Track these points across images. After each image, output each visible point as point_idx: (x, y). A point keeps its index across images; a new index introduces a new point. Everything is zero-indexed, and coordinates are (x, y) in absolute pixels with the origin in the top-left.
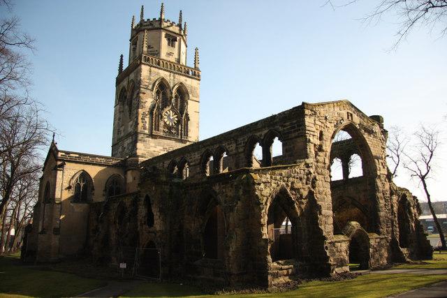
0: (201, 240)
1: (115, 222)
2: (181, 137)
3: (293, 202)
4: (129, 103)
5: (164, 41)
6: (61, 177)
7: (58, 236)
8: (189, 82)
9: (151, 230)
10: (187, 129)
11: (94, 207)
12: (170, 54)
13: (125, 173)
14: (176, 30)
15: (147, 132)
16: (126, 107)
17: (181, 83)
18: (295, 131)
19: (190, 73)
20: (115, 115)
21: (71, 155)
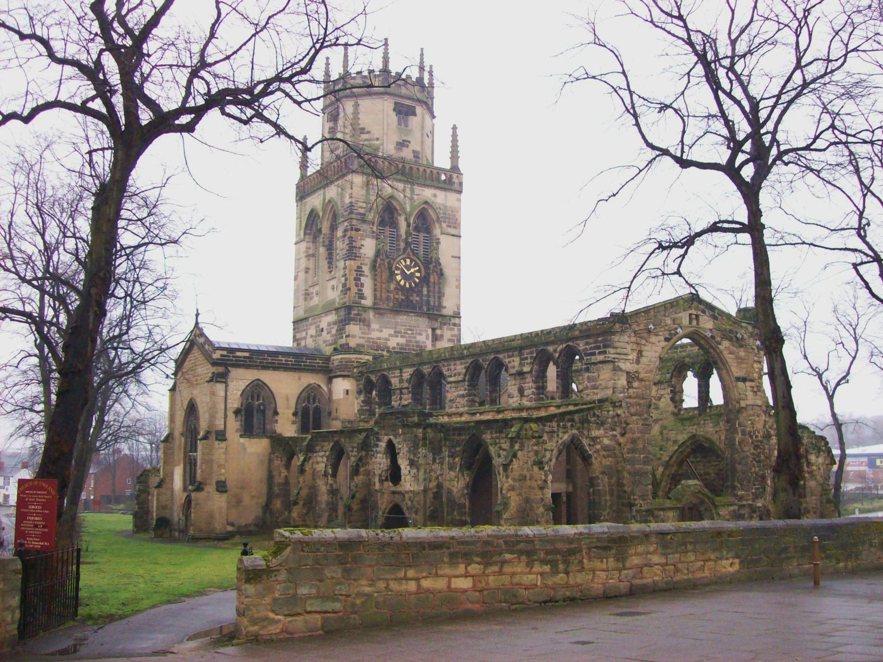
0: (467, 504)
1: (326, 474)
2: (428, 310)
3: (590, 456)
4: (327, 243)
5: (393, 117)
6: (222, 394)
7: (225, 495)
8: (440, 198)
9: (398, 488)
10: (439, 292)
11: (279, 443)
13: (330, 381)
15: (368, 302)
16: (322, 250)
17: (426, 203)
18: (600, 353)
19: (443, 177)
20: (298, 260)
21: (238, 354)
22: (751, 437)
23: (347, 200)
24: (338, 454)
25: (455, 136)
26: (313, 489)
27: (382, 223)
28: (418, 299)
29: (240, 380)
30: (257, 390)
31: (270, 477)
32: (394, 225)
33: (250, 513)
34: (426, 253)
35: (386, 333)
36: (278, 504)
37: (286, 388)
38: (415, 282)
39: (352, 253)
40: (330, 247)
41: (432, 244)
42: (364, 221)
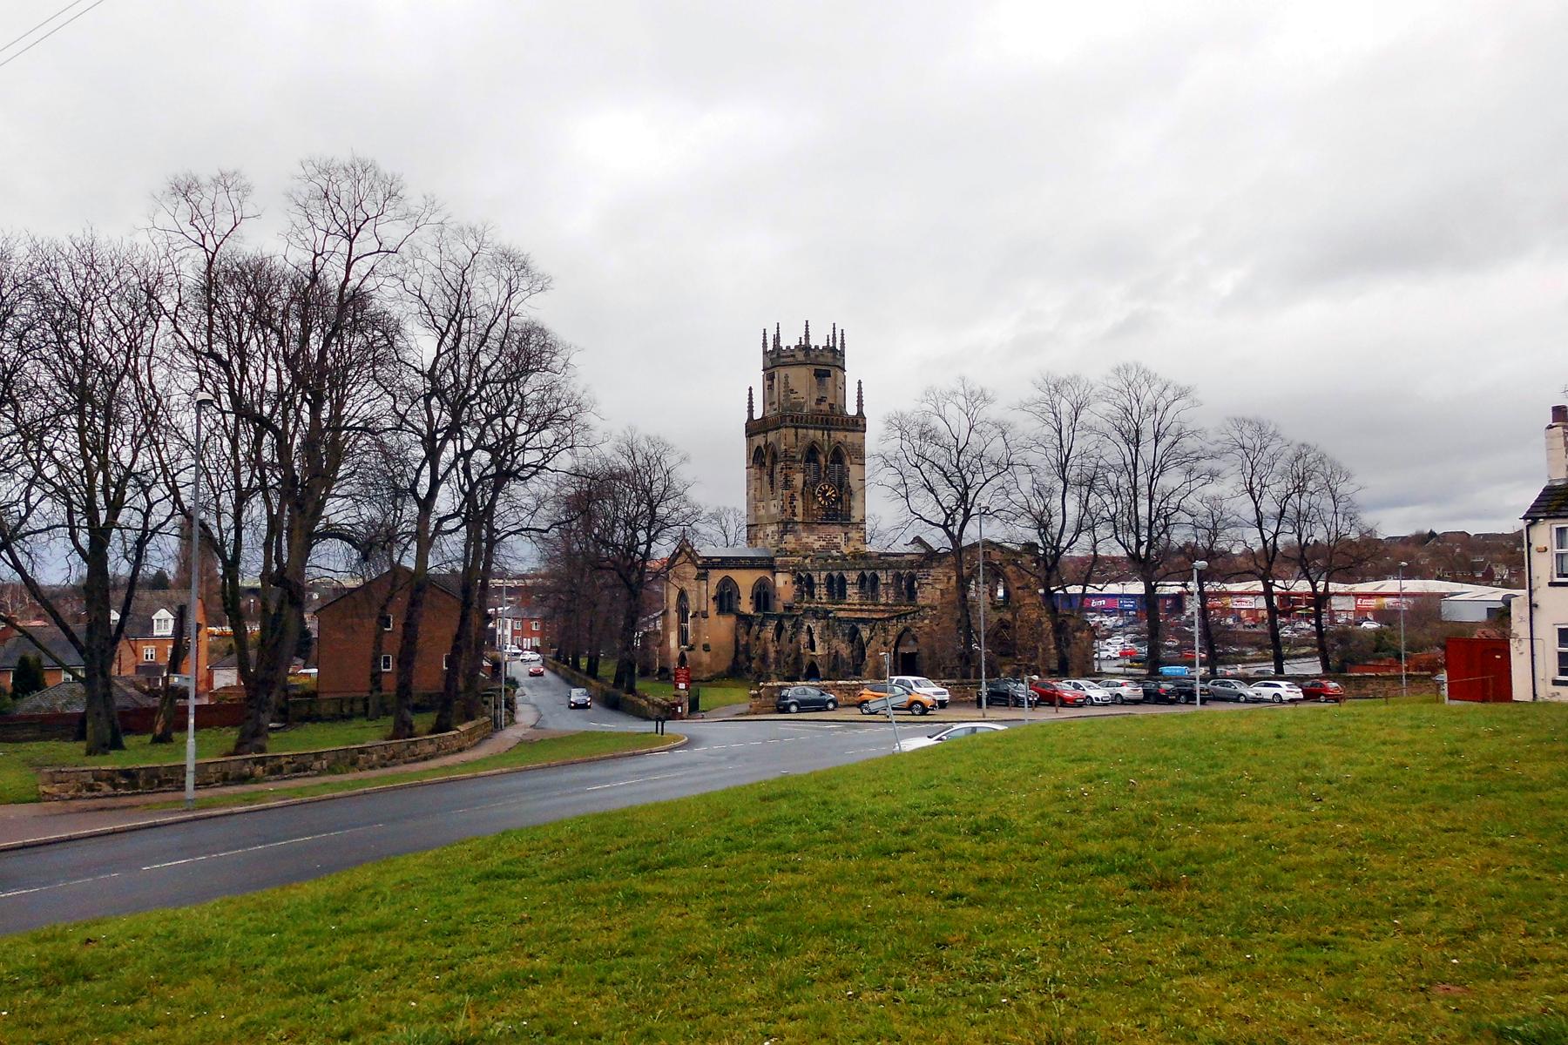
12: (820, 401)
14: (829, 357)
16: (766, 478)
23: (783, 447)
24: (779, 629)
25: (860, 388)
26: (765, 651)
27: (808, 461)
29: (716, 576)
30: (727, 581)
31: (737, 641)
32: (816, 461)
33: (725, 664)
34: (840, 479)
35: (812, 538)
36: (742, 657)
37: (745, 580)
39: (787, 484)
40: (771, 476)
41: (844, 474)
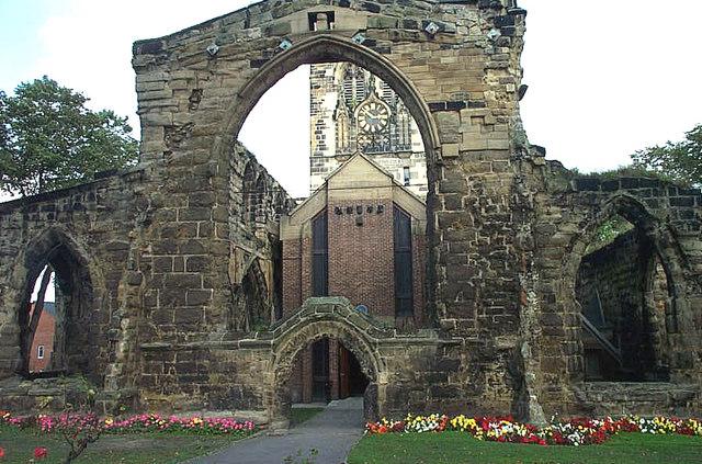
2: (397, 149)
22: (474, 211)
28: (386, 140)
38: (382, 125)
42: (322, 76)
